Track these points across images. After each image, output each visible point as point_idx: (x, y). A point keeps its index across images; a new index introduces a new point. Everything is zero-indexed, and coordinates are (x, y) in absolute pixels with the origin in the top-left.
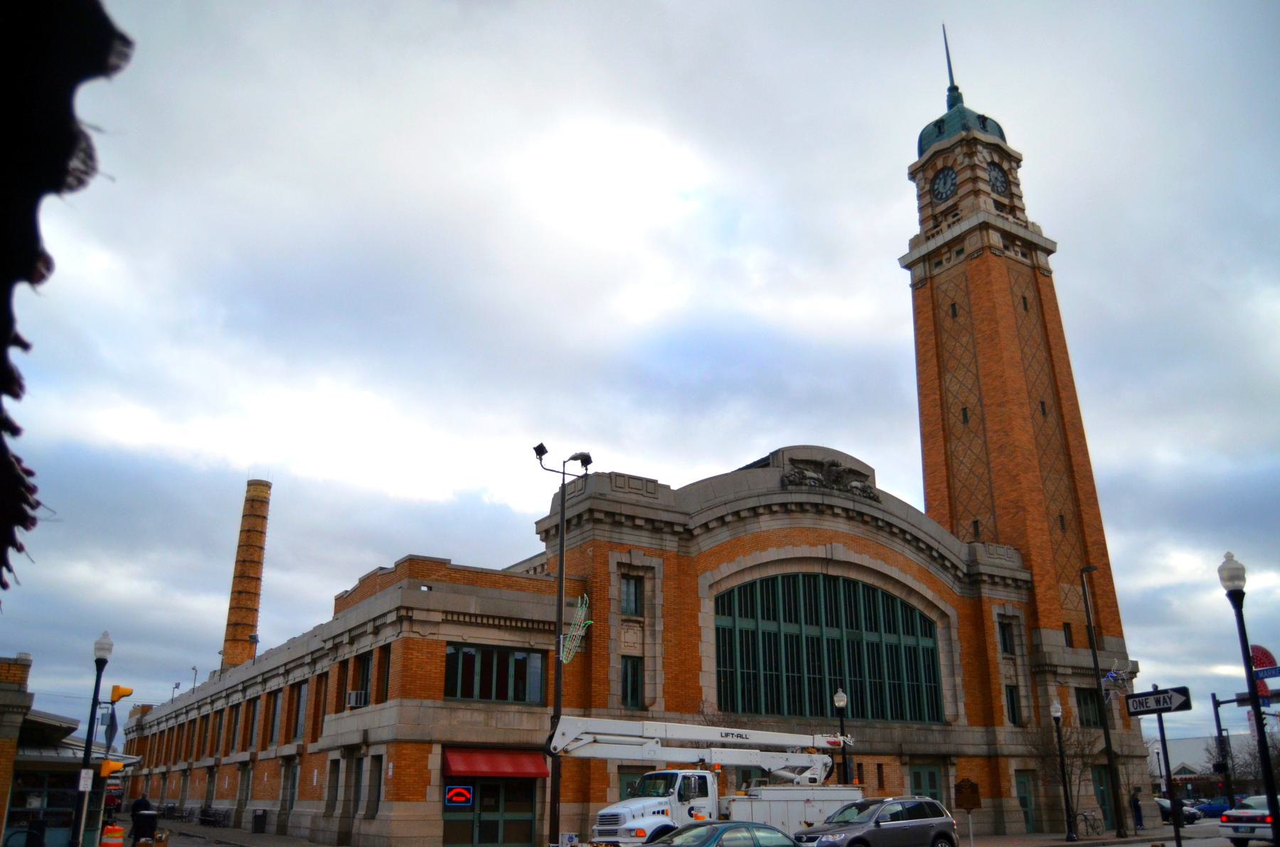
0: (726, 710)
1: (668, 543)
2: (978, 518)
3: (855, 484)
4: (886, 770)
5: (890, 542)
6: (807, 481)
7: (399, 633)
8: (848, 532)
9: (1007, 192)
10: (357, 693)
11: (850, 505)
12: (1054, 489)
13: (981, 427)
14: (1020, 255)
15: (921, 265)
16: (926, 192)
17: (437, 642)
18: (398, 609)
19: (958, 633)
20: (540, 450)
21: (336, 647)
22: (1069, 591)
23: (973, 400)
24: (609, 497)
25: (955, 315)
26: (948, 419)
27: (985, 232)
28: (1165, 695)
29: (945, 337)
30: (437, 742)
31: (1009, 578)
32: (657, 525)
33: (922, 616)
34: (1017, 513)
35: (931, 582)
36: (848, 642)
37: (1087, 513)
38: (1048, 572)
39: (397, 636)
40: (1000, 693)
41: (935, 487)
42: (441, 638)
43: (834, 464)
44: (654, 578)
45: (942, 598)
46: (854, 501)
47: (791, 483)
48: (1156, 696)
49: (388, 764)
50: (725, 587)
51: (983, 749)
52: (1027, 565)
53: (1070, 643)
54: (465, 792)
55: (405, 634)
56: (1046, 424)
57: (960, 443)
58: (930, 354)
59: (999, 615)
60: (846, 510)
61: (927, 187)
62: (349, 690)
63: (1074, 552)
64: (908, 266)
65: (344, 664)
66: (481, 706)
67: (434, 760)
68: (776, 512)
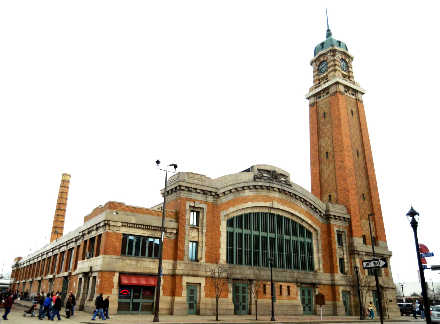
0: (230, 263)
1: (209, 199)
2: (331, 194)
3: (282, 179)
4: (291, 288)
5: (295, 202)
6: (264, 178)
7: (105, 230)
8: (279, 197)
9: (347, 70)
10: (89, 253)
11: (280, 187)
12: (360, 184)
13: (333, 159)
14: (351, 94)
15: (313, 98)
16: (316, 70)
17: (119, 234)
18: (104, 221)
19: (321, 237)
20: (158, 162)
21: (83, 235)
22: (365, 223)
23: (330, 149)
24: (187, 181)
25: (325, 117)
26: (321, 156)
27: (337, 85)
28: (378, 261)
29: (321, 125)
30: (117, 271)
31: (341, 217)
32: (205, 192)
33: (307, 230)
34: (345, 192)
35: (311, 217)
36: (278, 239)
37: (373, 194)
38: (357, 215)
39: (104, 231)
40: (337, 261)
41: (315, 182)
42: (121, 232)
43: (274, 172)
44: (203, 212)
45: (315, 224)
46: (282, 186)
47: (258, 178)
48: (374, 262)
49: (98, 280)
50: (231, 216)
51: (329, 282)
52: (349, 212)
53: (365, 243)
54: (127, 291)
55: (106, 230)
56: (358, 159)
57: (325, 166)
59: (337, 231)
60: (279, 189)
61: (317, 68)
62: (87, 251)
63: (368, 208)
64: (308, 98)
65: (86, 241)
66: (135, 258)
67: (116, 279)
68: (251, 189)
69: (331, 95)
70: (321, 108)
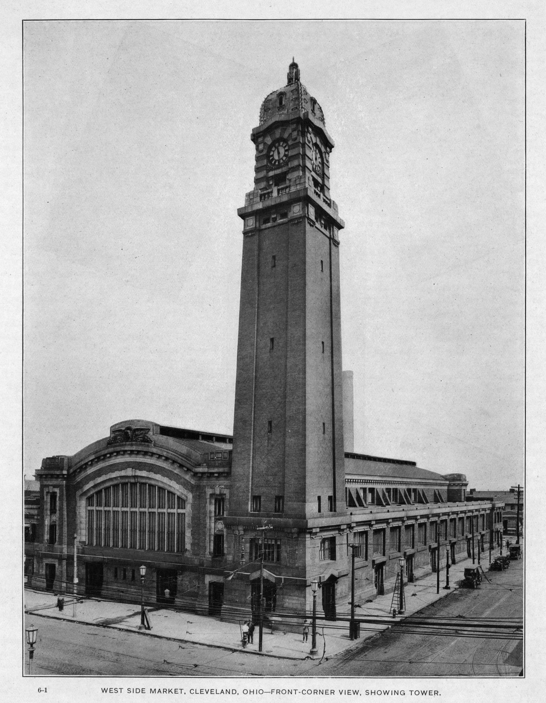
16: (263, 155)
64: (243, 214)
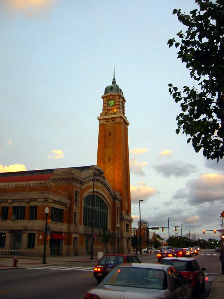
11: (102, 180)
15: (103, 120)
25: (110, 135)
44: (79, 194)
58: (102, 142)
64: (99, 120)
69: (116, 123)
70: (108, 129)
